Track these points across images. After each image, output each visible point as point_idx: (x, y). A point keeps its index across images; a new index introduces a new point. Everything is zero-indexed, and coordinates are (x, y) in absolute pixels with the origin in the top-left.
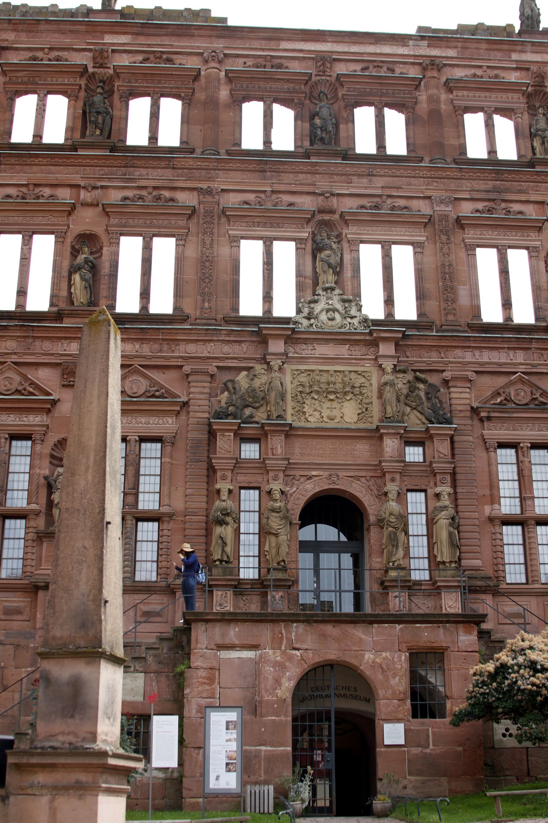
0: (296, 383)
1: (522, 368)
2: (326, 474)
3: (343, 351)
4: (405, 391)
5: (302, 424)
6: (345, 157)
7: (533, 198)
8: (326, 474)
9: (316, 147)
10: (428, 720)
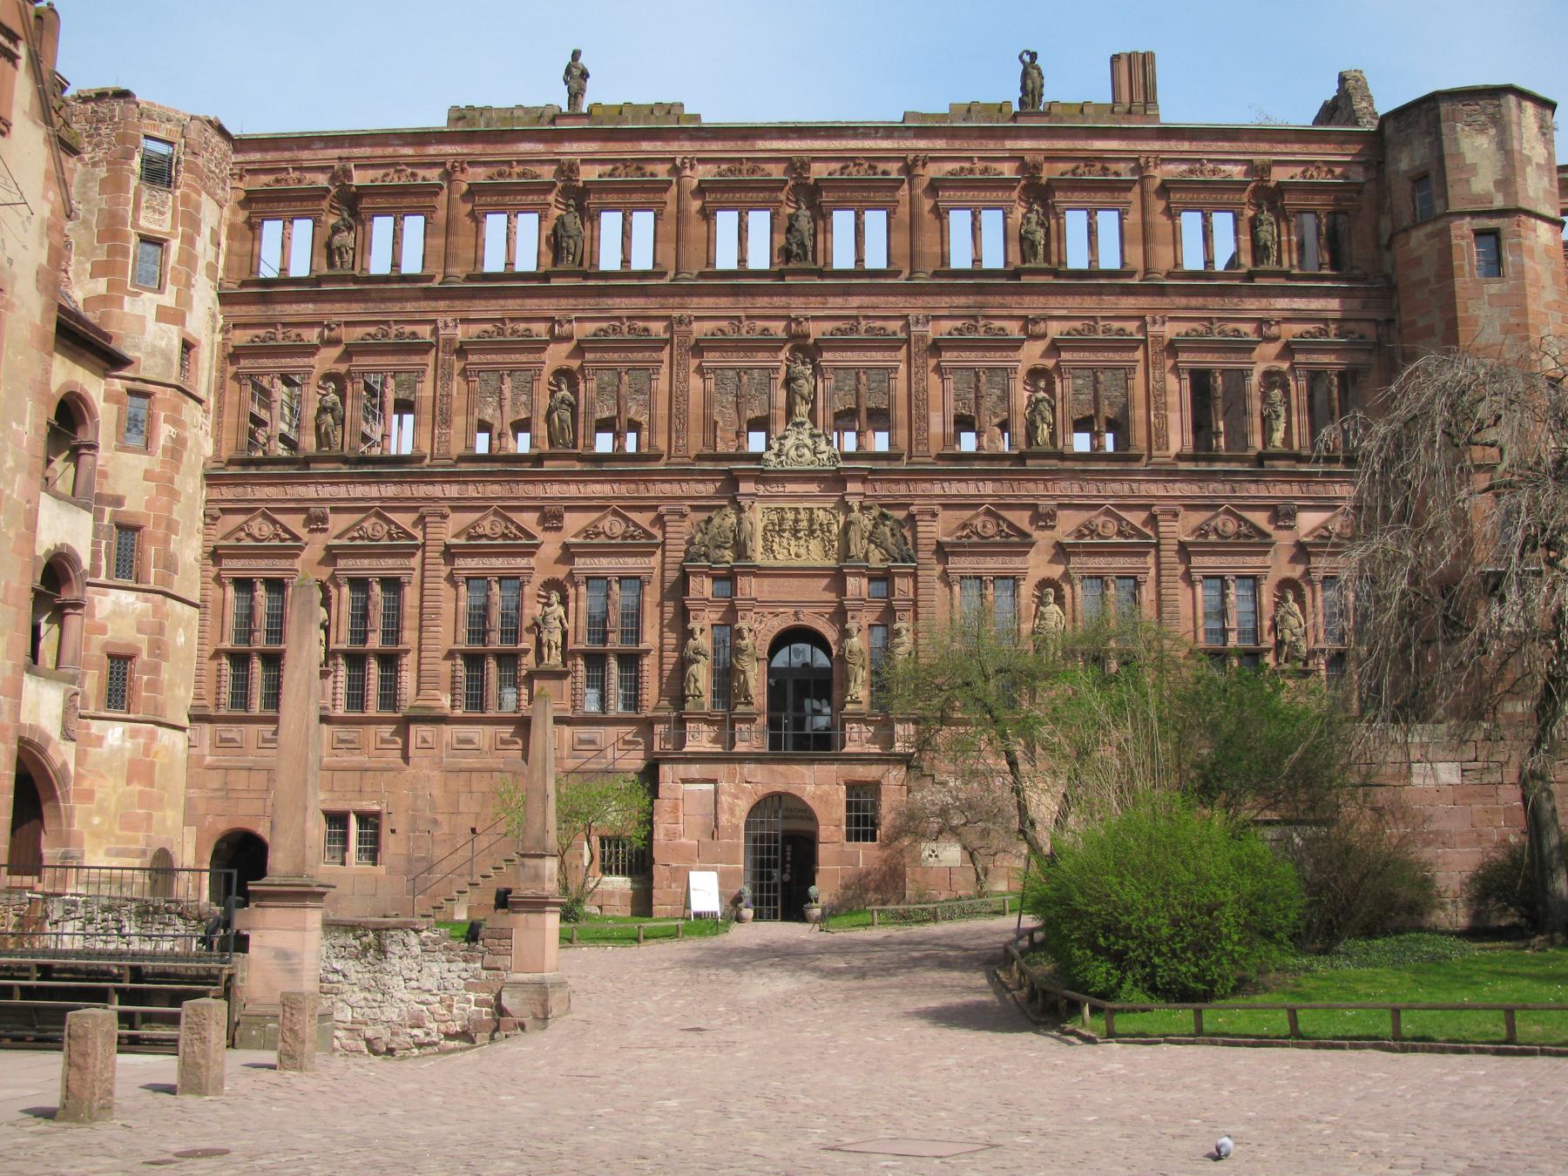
0: (765, 521)
1: (990, 500)
2: (792, 611)
3: (813, 488)
4: (870, 527)
5: (771, 563)
6: (821, 274)
7: (1016, 312)
8: (792, 611)
9: (791, 265)
10: (862, 843)
